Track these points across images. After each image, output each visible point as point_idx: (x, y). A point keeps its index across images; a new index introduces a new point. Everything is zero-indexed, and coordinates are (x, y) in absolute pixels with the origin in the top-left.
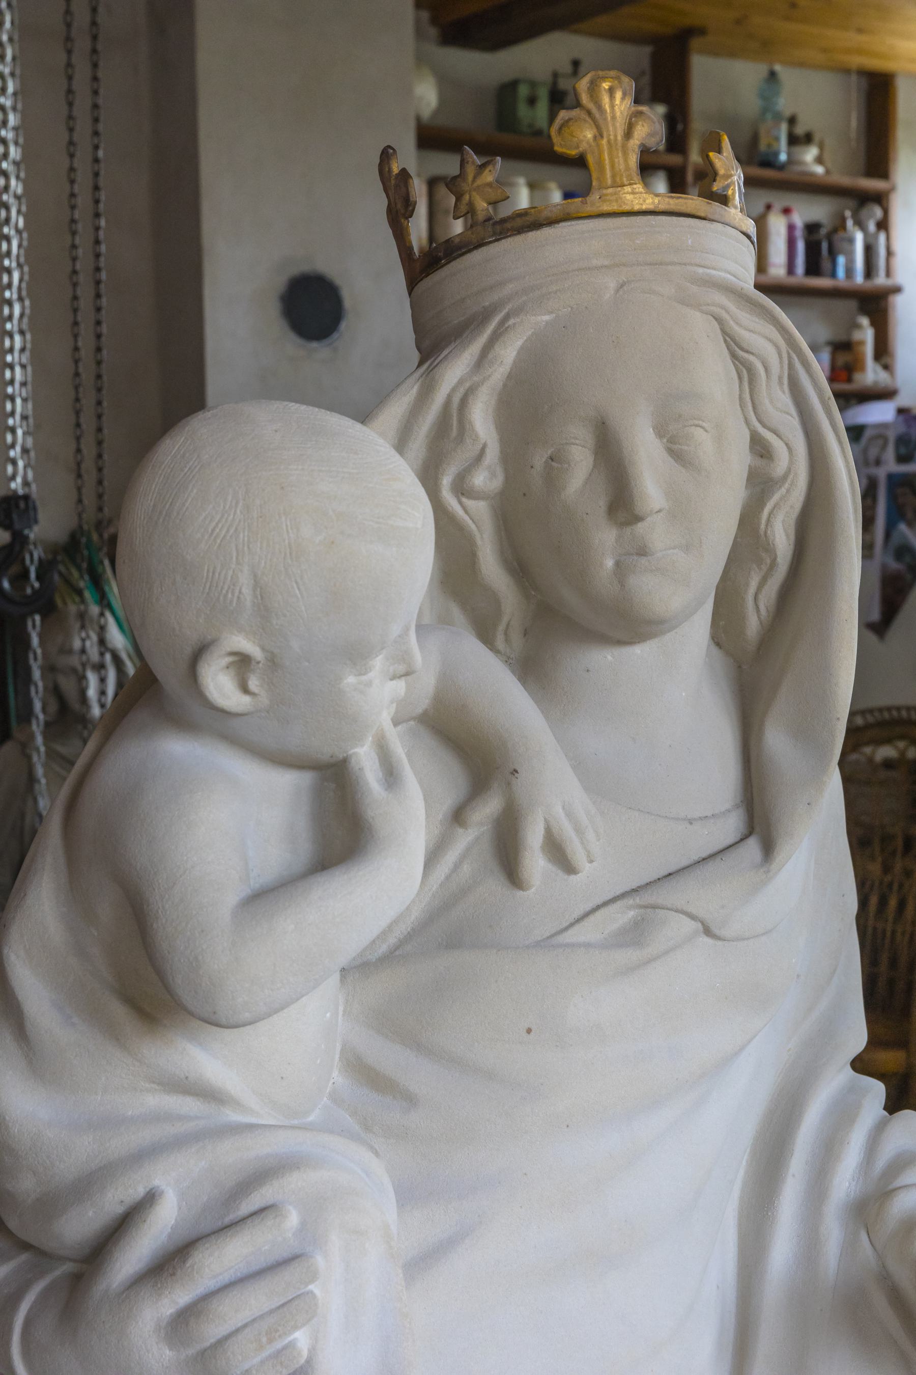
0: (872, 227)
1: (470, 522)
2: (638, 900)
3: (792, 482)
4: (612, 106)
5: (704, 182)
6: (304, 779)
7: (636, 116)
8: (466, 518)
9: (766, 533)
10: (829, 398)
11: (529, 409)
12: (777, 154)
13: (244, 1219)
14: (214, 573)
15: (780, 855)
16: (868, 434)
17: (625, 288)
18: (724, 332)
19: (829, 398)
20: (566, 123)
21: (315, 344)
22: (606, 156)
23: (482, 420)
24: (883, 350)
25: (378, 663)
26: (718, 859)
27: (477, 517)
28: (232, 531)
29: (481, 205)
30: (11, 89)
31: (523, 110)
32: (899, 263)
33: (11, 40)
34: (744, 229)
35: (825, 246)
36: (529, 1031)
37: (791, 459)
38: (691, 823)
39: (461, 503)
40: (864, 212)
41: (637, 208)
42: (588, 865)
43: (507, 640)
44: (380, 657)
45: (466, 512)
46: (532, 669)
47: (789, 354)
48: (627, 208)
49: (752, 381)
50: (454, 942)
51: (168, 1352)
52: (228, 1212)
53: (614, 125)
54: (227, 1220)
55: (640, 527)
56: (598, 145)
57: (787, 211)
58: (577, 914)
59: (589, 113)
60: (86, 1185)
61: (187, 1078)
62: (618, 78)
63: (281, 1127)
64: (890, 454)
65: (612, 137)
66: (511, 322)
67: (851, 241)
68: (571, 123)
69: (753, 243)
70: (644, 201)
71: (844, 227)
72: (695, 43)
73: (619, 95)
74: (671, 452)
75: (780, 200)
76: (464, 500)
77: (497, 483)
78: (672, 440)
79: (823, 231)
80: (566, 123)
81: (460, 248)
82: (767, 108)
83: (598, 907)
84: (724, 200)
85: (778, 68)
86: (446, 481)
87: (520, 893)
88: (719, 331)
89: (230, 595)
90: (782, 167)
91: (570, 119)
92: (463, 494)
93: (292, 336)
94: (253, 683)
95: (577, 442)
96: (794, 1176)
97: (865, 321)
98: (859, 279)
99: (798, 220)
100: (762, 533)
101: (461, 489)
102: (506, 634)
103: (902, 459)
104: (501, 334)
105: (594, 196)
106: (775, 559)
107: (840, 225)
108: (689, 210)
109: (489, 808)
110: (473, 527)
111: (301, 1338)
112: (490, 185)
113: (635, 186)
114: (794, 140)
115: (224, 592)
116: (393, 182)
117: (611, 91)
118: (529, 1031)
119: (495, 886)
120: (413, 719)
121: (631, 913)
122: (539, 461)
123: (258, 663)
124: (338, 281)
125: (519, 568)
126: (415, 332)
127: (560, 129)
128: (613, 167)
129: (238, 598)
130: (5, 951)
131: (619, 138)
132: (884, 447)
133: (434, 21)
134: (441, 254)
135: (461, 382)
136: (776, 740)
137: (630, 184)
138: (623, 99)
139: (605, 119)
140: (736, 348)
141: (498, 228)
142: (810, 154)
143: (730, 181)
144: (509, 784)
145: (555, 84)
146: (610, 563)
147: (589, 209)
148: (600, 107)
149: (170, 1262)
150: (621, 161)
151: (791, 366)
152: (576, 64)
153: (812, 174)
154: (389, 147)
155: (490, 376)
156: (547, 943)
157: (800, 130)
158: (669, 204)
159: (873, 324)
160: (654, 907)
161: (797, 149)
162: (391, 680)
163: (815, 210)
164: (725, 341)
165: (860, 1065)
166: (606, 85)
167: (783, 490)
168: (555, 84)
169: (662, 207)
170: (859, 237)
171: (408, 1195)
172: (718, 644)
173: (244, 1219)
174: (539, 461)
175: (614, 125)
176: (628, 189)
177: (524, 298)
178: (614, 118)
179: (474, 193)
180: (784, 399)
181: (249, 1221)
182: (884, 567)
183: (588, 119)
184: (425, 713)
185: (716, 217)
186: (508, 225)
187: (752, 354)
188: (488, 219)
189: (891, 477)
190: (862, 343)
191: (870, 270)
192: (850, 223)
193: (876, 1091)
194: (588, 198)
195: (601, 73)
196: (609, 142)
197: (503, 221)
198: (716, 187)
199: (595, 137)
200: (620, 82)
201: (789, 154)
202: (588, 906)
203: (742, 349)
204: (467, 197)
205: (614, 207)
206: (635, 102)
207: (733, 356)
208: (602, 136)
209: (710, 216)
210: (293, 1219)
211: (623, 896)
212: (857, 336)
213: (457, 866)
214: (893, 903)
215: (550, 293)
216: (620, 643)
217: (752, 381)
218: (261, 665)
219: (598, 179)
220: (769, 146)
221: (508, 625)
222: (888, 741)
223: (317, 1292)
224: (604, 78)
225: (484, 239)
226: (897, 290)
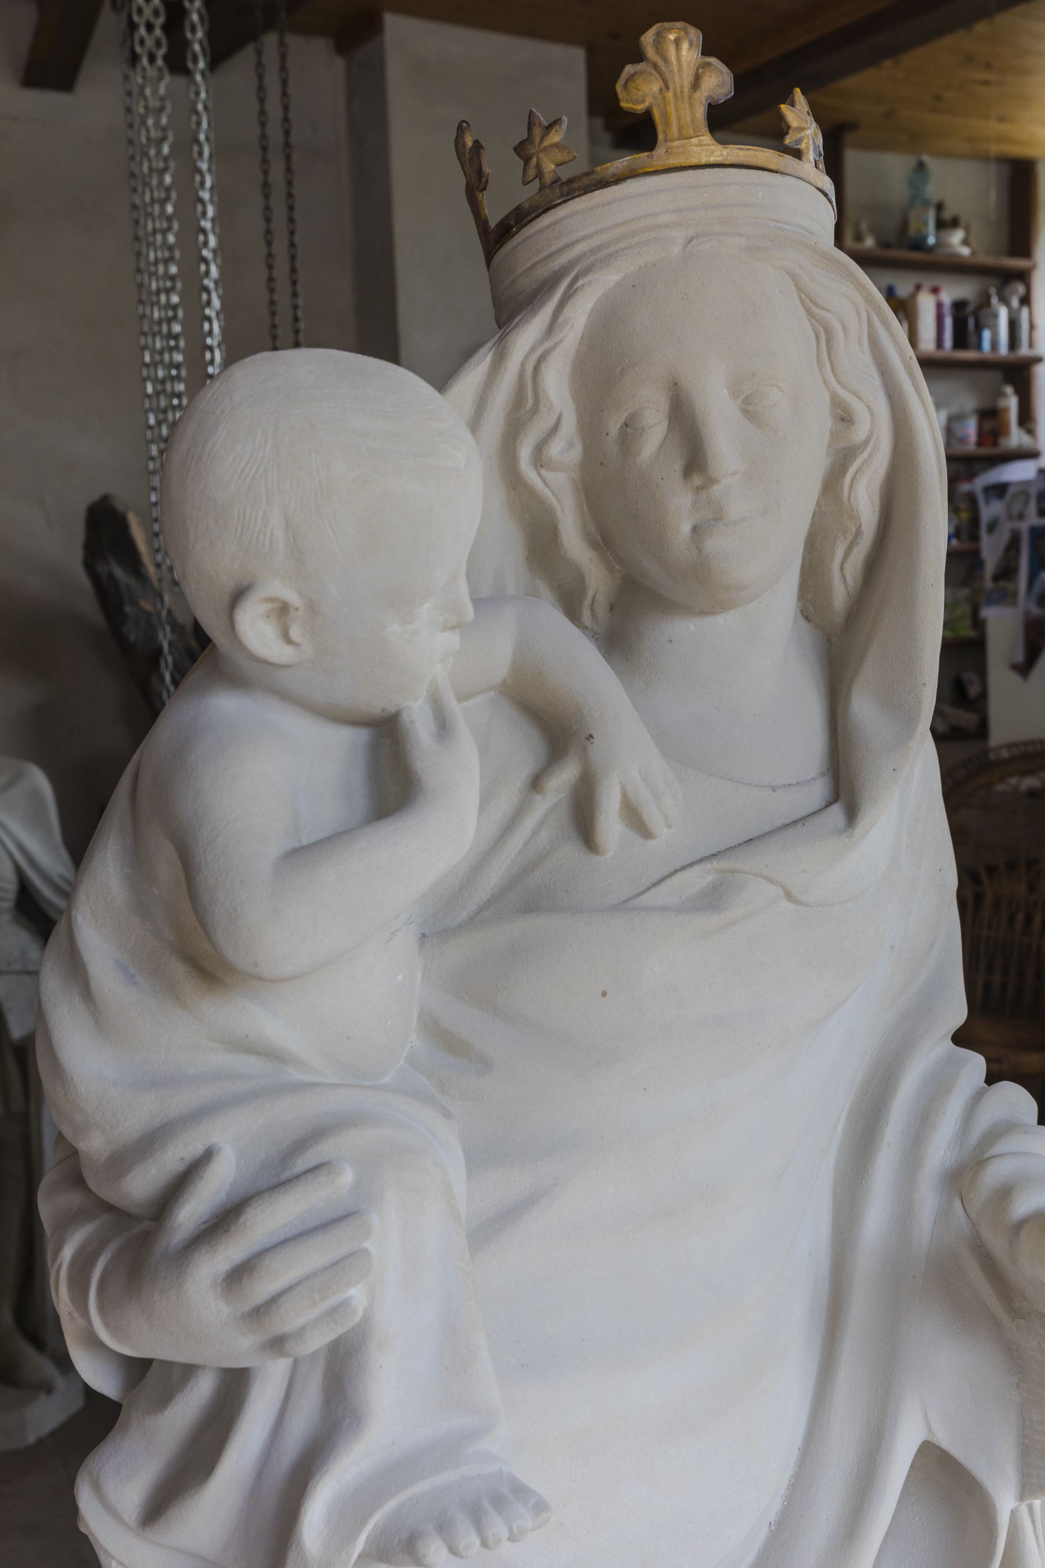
0: (1015, 302)
1: (550, 495)
2: (716, 864)
3: (875, 445)
4: (679, 57)
5: (775, 135)
6: (361, 736)
7: (703, 67)
8: (546, 491)
9: (849, 499)
10: (911, 358)
11: (602, 373)
12: (924, 239)
13: (298, 1177)
14: (244, 514)
15: (864, 821)
16: (1012, 490)
17: (694, 243)
18: (799, 289)
19: (911, 358)
20: (632, 77)
22: (671, 109)
23: (557, 385)
24: (1026, 417)
25: (425, 610)
26: (800, 825)
27: (558, 489)
28: (261, 470)
29: (549, 167)
30: (208, 183)
33: (207, 139)
34: (820, 186)
35: (971, 323)
36: (604, 994)
37: (873, 424)
38: (774, 790)
39: (540, 475)
40: (1008, 290)
41: (704, 160)
42: (665, 830)
43: (594, 616)
44: (426, 606)
45: (546, 484)
46: (618, 640)
47: (868, 312)
48: (694, 161)
49: (829, 340)
50: (530, 906)
51: (225, 1308)
52: (281, 1171)
53: (681, 77)
54: (283, 1177)
55: (716, 490)
56: (664, 98)
57: (935, 291)
58: (654, 878)
59: (655, 66)
60: (149, 1143)
61: (247, 1036)
62: (685, 29)
63: (340, 1085)
64: (1032, 508)
65: (678, 89)
66: (580, 283)
67: (996, 316)
68: (636, 77)
69: (830, 202)
70: (712, 153)
72: (849, 137)
73: (685, 46)
74: (745, 412)
75: (928, 280)
76: (543, 472)
77: (576, 454)
78: (747, 401)
79: (970, 309)
80: (632, 77)
81: (530, 214)
82: (916, 197)
83: (676, 871)
84: (797, 154)
85: (926, 158)
86: (525, 453)
87: (596, 858)
88: (793, 289)
89: (262, 537)
90: (930, 250)
91: (635, 74)
92: (541, 466)
94: (295, 633)
95: (651, 405)
96: (889, 1145)
97: (1009, 390)
98: (1003, 350)
99: (947, 297)
100: (845, 499)
101: (539, 459)
102: (592, 610)
103: (1044, 512)
104: (570, 297)
105: (660, 150)
106: (860, 527)
107: (985, 302)
108: (759, 163)
109: (566, 775)
110: (553, 499)
111: (357, 1294)
112: (556, 145)
113: (702, 138)
114: (942, 225)
115: (256, 534)
116: (467, 156)
117: (677, 42)
118: (604, 994)
119: (572, 851)
120: (492, 688)
121: (710, 878)
122: (614, 424)
123: (297, 609)
125: (604, 540)
126: (494, 307)
127: (626, 83)
128: (679, 119)
129: (271, 540)
130: (73, 913)
131: (686, 90)
132: (1026, 502)
133: (608, 127)
134: (512, 222)
135: (533, 349)
136: (863, 708)
137: (697, 136)
138: (689, 50)
139: (671, 71)
140: (813, 307)
141: (565, 189)
142: (956, 238)
143: (803, 134)
144: (585, 749)
146: (686, 528)
147: (658, 164)
148: (665, 60)
149: (224, 1220)
150: (688, 114)
151: (870, 324)
154: (464, 121)
155: (561, 341)
156: (624, 906)
157: (947, 215)
158: (738, 156)
159: (1018, 392)
160: (733, 872)
162: (443, 631)
164: (800, 298)
165: (961, 1038)
166: (672, 37)
167: (865, 454)
169: (731, 160)
171: (480, 1158)
172: (807, 618)
173: (298, 1177)
174: (614, 424)
175: (681, 77)
176: (695, 141)
177: (592, 259)
178: (680, 69)
179: (542, 155)
180: (866, 359)
181: (303, 1178)
182: (1027, 613)
183: (653, 72)
184: (504, 683)
185: (788, 171)
186: (575, 185)
187: (829, 311)
188: (556, 180)
189: (1034, 531)
190: (1007, 410)
191: (1014, 341)
192: (994, 300)
193: (976, 1064)
194: (654, 153)
195: (666, 25)
196: (675, 94)
197: (570, 181)
198: (788, 141)
199: (661, 90)
200: (686, 33)
201: (937, 238)
202: (666, 871)
203: (817, 305)
204: (534, 160)
205: (681, 161)
206: (702, 54)
207: (810, 313)
208: (667, 88)
209: (783, 170)
210: (347, 1177)
211: (701, 861)
212: (1002, 403)
213: (535, 833)
215: (618, 251)
216: (702, 613)
217: (829, 340)
218: (300, 612)
219: (665, 132)
221: (593, 600)
222: (1032, 772)
223: (372, 1250)
224: (669, 30)
225: (552, 201)
226: (1038, 360)
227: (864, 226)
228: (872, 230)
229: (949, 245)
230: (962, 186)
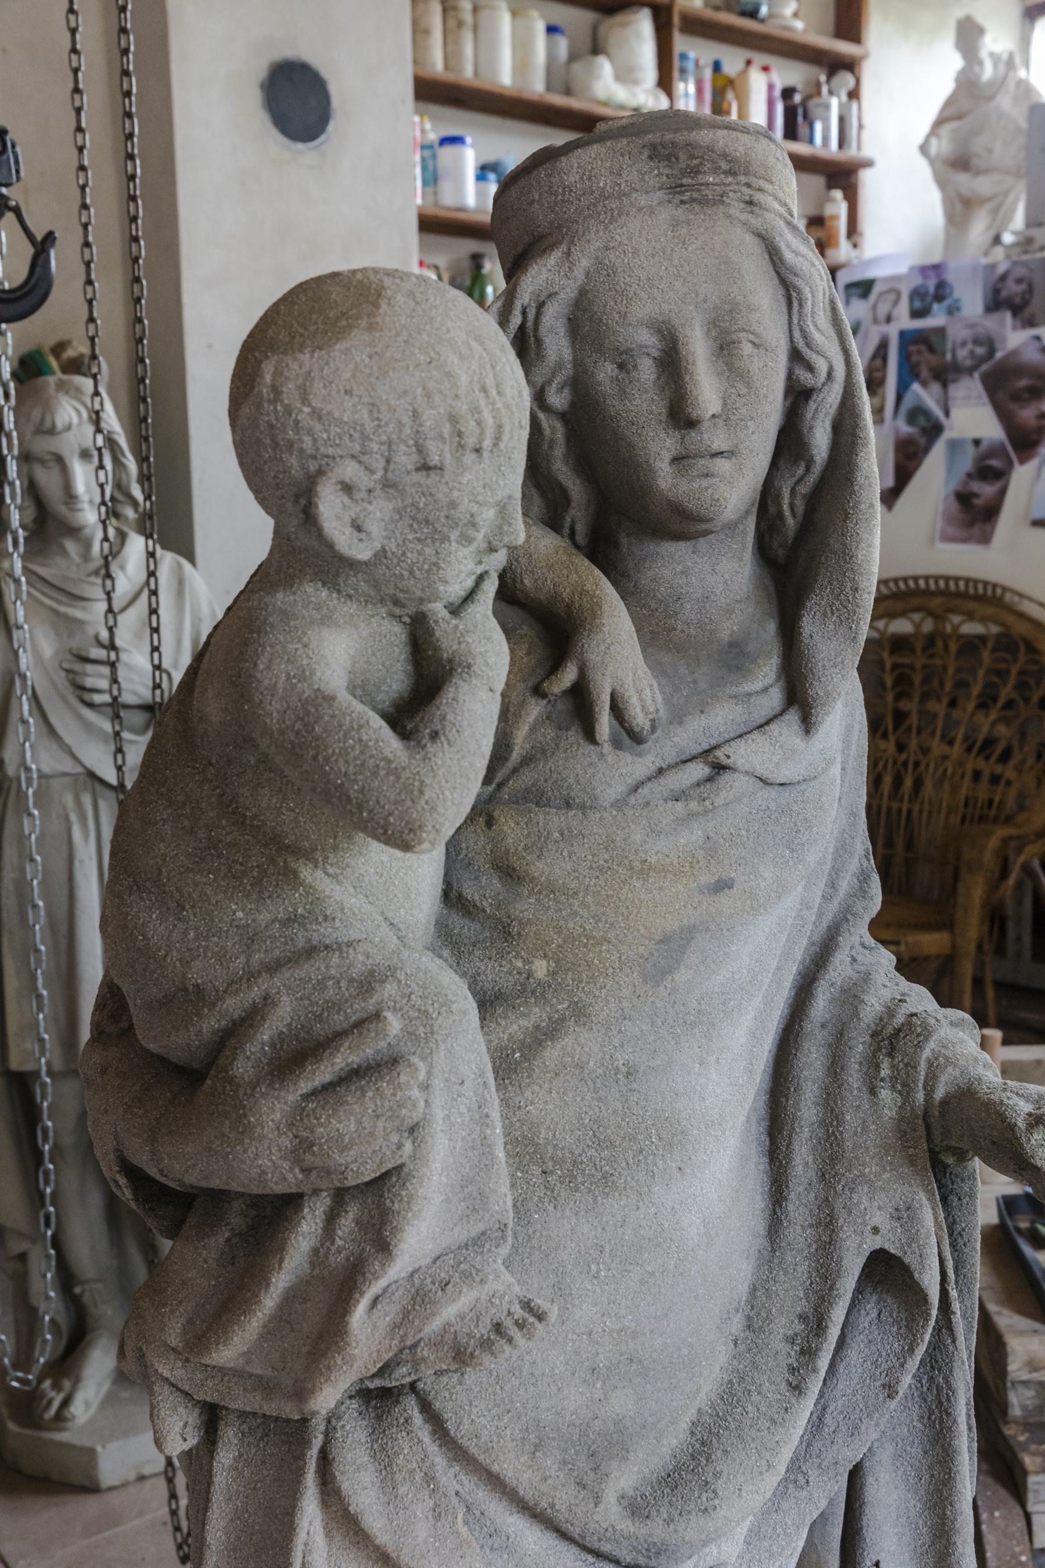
21: (300, 146)
24: (853, 229)
40: (837, 80)
57: (766, 69)
64: (903, 309)
67: (827, 107)
71: (819, 93)
90: (762, 21)
93: (275, 133)
97: (838, 194)
103: (916, 314)
124: (325, 74)
132: (896, 303)
163: (788, 74)
182: (897, 431)
189: (902, 334)
190: (835, 217)
212: (829, 210)
214: (908, 782)
222: (903, 614)
226: (868, 164)
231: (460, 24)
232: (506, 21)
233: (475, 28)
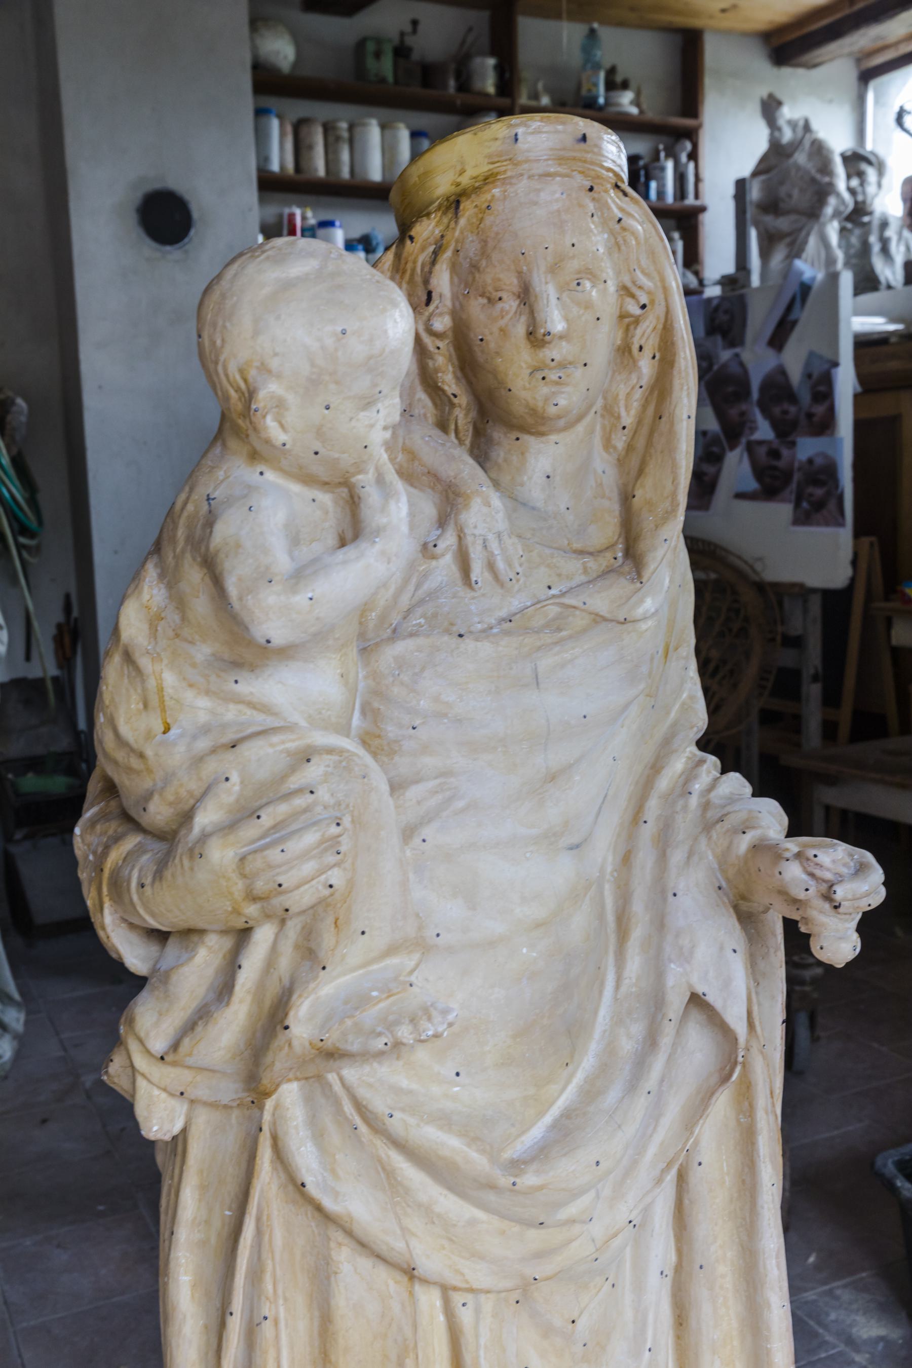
0: (684, 158)
12: (596, 98)
21: (168, 248)
31: (370, 63)
32: (705, 187)
35: (642, 173)
40: (678, 147)
67: (663, 169)
79: (641, 163)
85: (595, 25)
90: (601, 109)
98: (670, 198)
107: (656, 158)
114: (611, 85)
124: (187, 197)
145: (402, 41)
152: (415, 23)
153: (627, 114)
159: (683, 237)
161: (613, 94)
168: (402, 41)
170: (670, 165)
191: (681, 192)
192: (662, 155)
201: (606, 99)
220: (589, 91)
227: (540, 86)
228: (549, 91)
229: (619, 105)
230: (633, 51)
231: (338, 139)
232: (374, 134)
233: (351, 142)
